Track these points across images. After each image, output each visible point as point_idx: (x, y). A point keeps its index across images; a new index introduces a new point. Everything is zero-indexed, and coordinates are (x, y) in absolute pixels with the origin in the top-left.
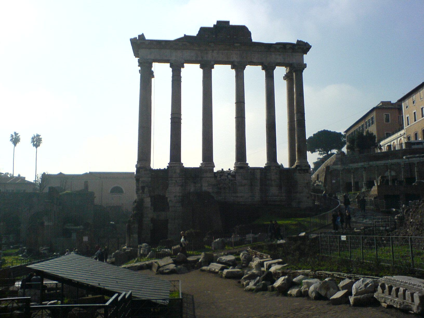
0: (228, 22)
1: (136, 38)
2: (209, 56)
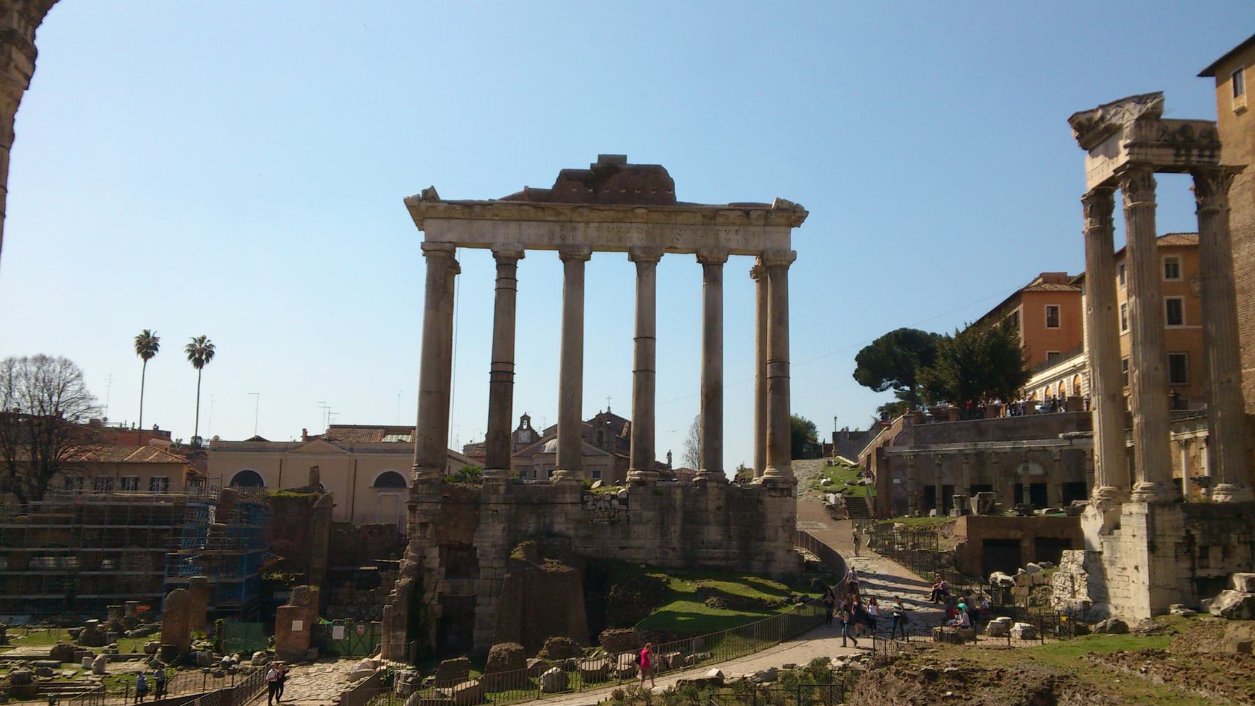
0: (625, 157)
1: (417, 198)
2: (580, 235)
